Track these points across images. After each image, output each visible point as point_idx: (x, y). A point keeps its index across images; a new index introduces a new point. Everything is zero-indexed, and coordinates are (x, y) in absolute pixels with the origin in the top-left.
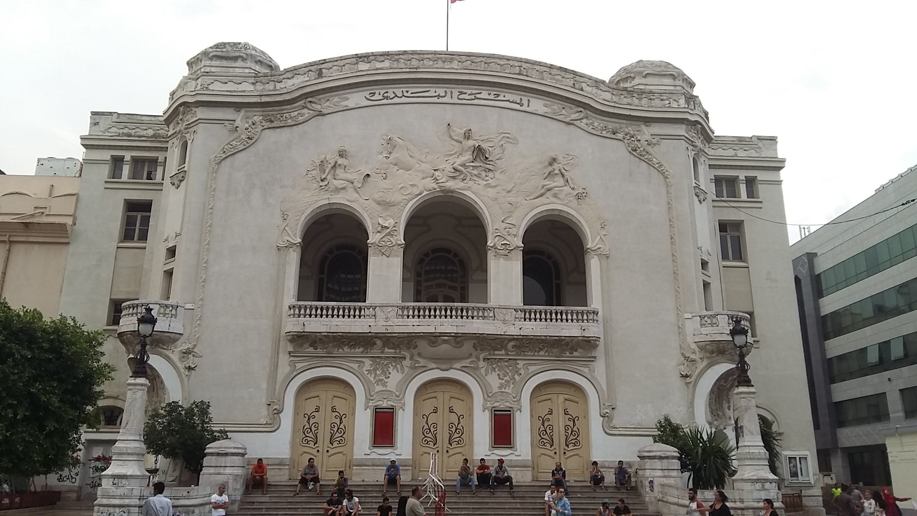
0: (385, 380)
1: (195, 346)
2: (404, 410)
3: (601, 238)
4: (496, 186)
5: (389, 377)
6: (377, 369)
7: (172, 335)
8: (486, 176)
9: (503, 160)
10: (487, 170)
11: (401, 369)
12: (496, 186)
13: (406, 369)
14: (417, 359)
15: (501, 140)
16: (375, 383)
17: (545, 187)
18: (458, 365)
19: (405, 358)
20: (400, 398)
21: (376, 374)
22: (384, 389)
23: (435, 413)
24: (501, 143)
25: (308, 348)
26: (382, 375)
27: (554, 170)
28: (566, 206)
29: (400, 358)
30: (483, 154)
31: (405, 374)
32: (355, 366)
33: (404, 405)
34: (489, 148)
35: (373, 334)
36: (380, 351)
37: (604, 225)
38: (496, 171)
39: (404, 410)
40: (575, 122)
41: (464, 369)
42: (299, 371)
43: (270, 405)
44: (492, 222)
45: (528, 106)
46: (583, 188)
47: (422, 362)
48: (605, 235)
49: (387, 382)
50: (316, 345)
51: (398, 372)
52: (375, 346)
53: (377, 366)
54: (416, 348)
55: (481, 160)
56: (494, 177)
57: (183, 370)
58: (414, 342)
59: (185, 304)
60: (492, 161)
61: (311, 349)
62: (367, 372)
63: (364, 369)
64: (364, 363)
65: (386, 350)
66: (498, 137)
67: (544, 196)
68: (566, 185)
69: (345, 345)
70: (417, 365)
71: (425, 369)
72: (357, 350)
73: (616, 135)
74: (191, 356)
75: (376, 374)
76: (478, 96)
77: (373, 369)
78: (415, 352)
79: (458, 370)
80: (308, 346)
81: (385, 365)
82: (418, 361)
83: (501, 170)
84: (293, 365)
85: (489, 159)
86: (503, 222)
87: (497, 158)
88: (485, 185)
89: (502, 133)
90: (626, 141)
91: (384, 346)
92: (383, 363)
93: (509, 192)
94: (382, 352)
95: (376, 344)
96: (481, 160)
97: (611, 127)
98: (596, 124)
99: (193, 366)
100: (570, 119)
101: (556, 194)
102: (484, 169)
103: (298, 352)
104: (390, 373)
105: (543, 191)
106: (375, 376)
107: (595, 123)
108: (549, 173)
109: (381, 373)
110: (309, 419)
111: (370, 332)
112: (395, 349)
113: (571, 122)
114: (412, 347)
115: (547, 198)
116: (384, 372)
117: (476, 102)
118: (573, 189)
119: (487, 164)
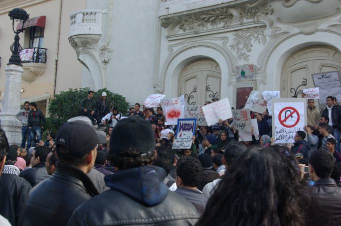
0: (247, 53)
1: (108, 44)
2: (265, 84)
5: (250, 51)
6: (240, 43)
7: (92, 37)
11: (262, 39)
13: (268, 39)
14: (277, 26)
16: (238, 58)
18: (324, 25)
19: (266, 26)
20: (261, 70)
21: (238, 49)
22: (246, 63)
23: (304, 85)
25: (179, 31)
26: (244, 49)
29: (263, 26)
31: (266, 44)
32: (220, 43)
33: (265, 78)
35: (225, 5)
36: (239, 22)
39: (265, 84)
41: (334, 29)
42: (175, 55)
43: (155, 87)
47: (283, 27)
49: (248, 56)
50: (184, 27)
51: (260, 43)
52: (234, 18)
53: (240, 40)
54: (273, 12)
57: (100, 64)
58: (269, 4)
59: (102, 9)
61: (181, 32)
62: (231, 47)
63: (228, 44)
64: (226, 38)
65: (245, 20)
69: (206, 22)
70: (278, 32)
71: (287, 35)
72: (219, 26)
74: (106, 52)
75: (238, 49)
77: (237, 43)
78: (272, 17)
79: (326, 31)
80: (179, 29)
81: (247, 38)
82: (280, 28)
84: (170, 48)
91: (241, 17)
92: (244, 36)
94: (242, 24)
95: (232, 15)
99: (107, 60)
103: (172, 36)
104: (251, 46)
106: (238, 52)
109: (244, 47)
110: (189, 99)
111: (222, 3)
112: (253, 18)
114: (268, 12)
116: (246, 45)
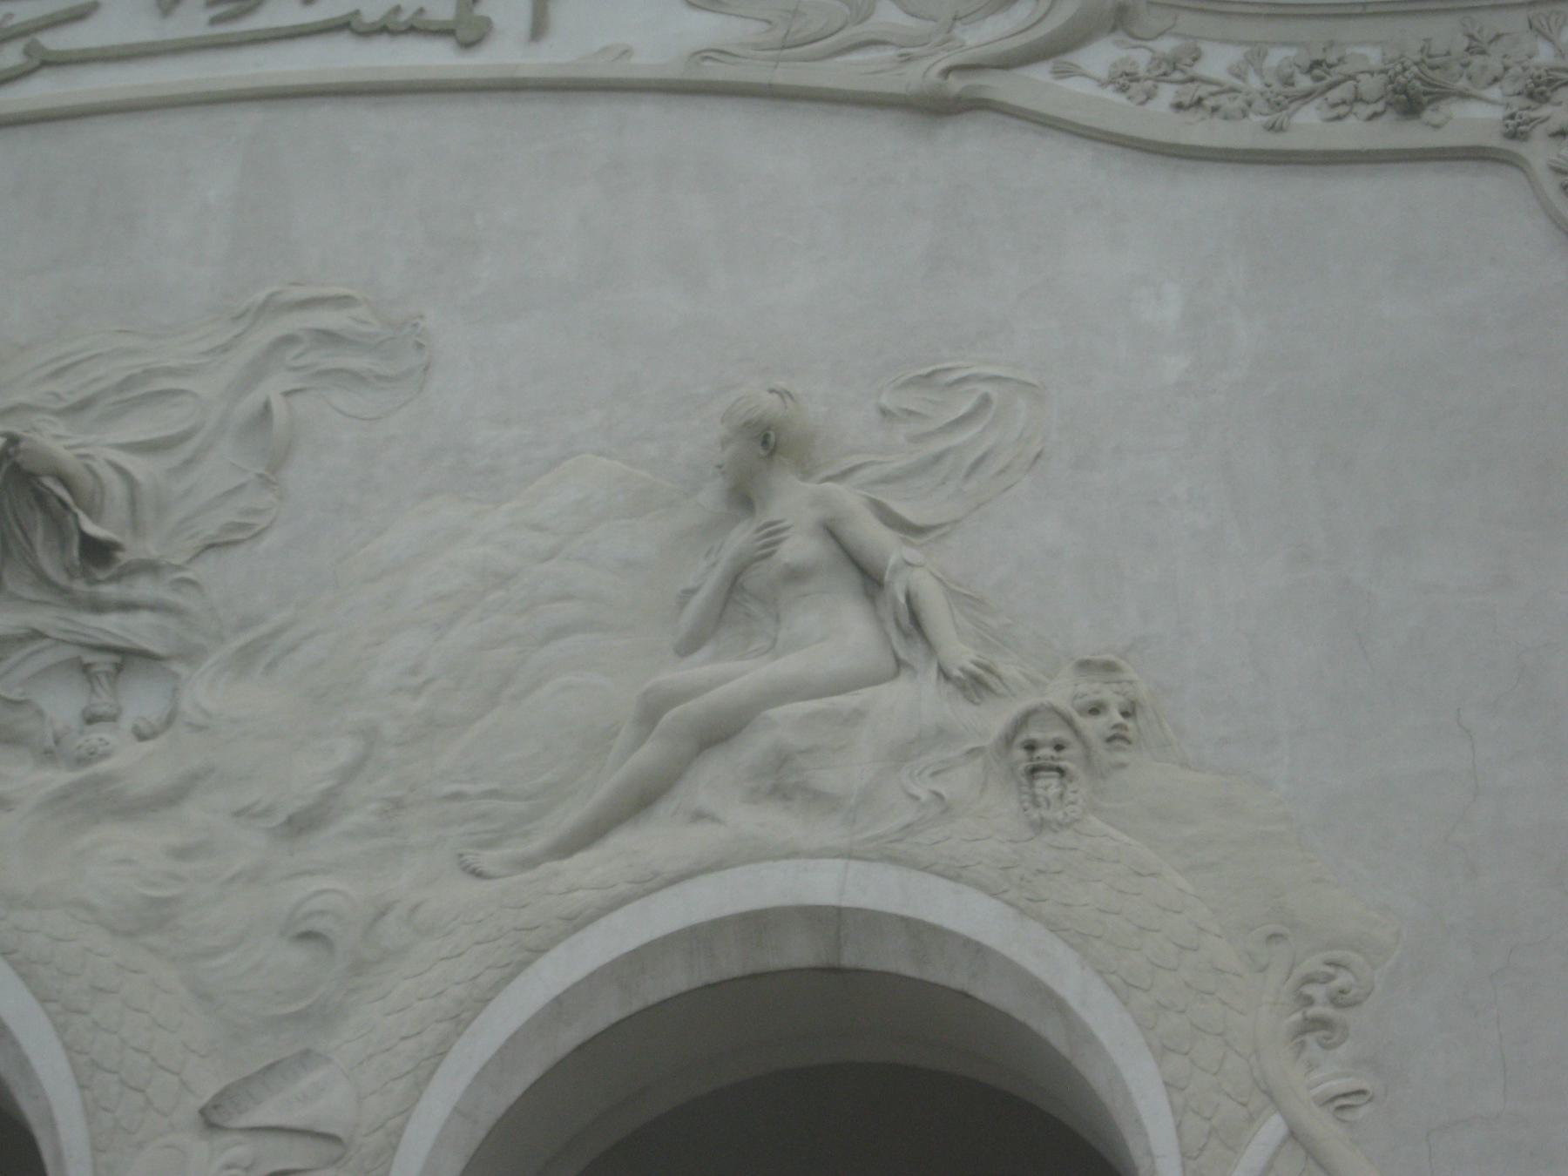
3: (1293, 1135)
4: (169, 799)
8: (91, 719)
9: (270, 541)
10: (103, 662)
12: (169, 799)
15: (255, 373)
17: (667, 717)
24: (250, 403)
27: (773, 535)
28: (894, 860)
30: (58, 517)
34: (122, 458)
37: (1339, 999)
38: (191, 655)
40: (1000, 86)
44: (96, 1149)
45: (539, 29)
46: (1085, 666)
48: (1340, 1103)
55: (43, 580)
56: (170, 721)
60: (150, 568)
66: (225, 349)
67: (664, 809)
68: (900, 664)
73: (1428, 115)
76: (54, 41)
83: (236, 643)
85: (123, 557)
86: (210, 1120)
87: (210, 527)
88: (61, 800)
89: (272, 307)
90: (1539, 152)
93: (301, 825)
96: (43, 580)
97: (1374, 56)
98: (1217, 62)
100: (957, 58)
101: (782, 759)
102: (70, 652)
105: (649, 754)
107: (1205, 46)
108: (734, 584)
113: (956, 85)
115: (699, 816)
117: (42, 91)
118: (975, 685)
119: (98, 607)
